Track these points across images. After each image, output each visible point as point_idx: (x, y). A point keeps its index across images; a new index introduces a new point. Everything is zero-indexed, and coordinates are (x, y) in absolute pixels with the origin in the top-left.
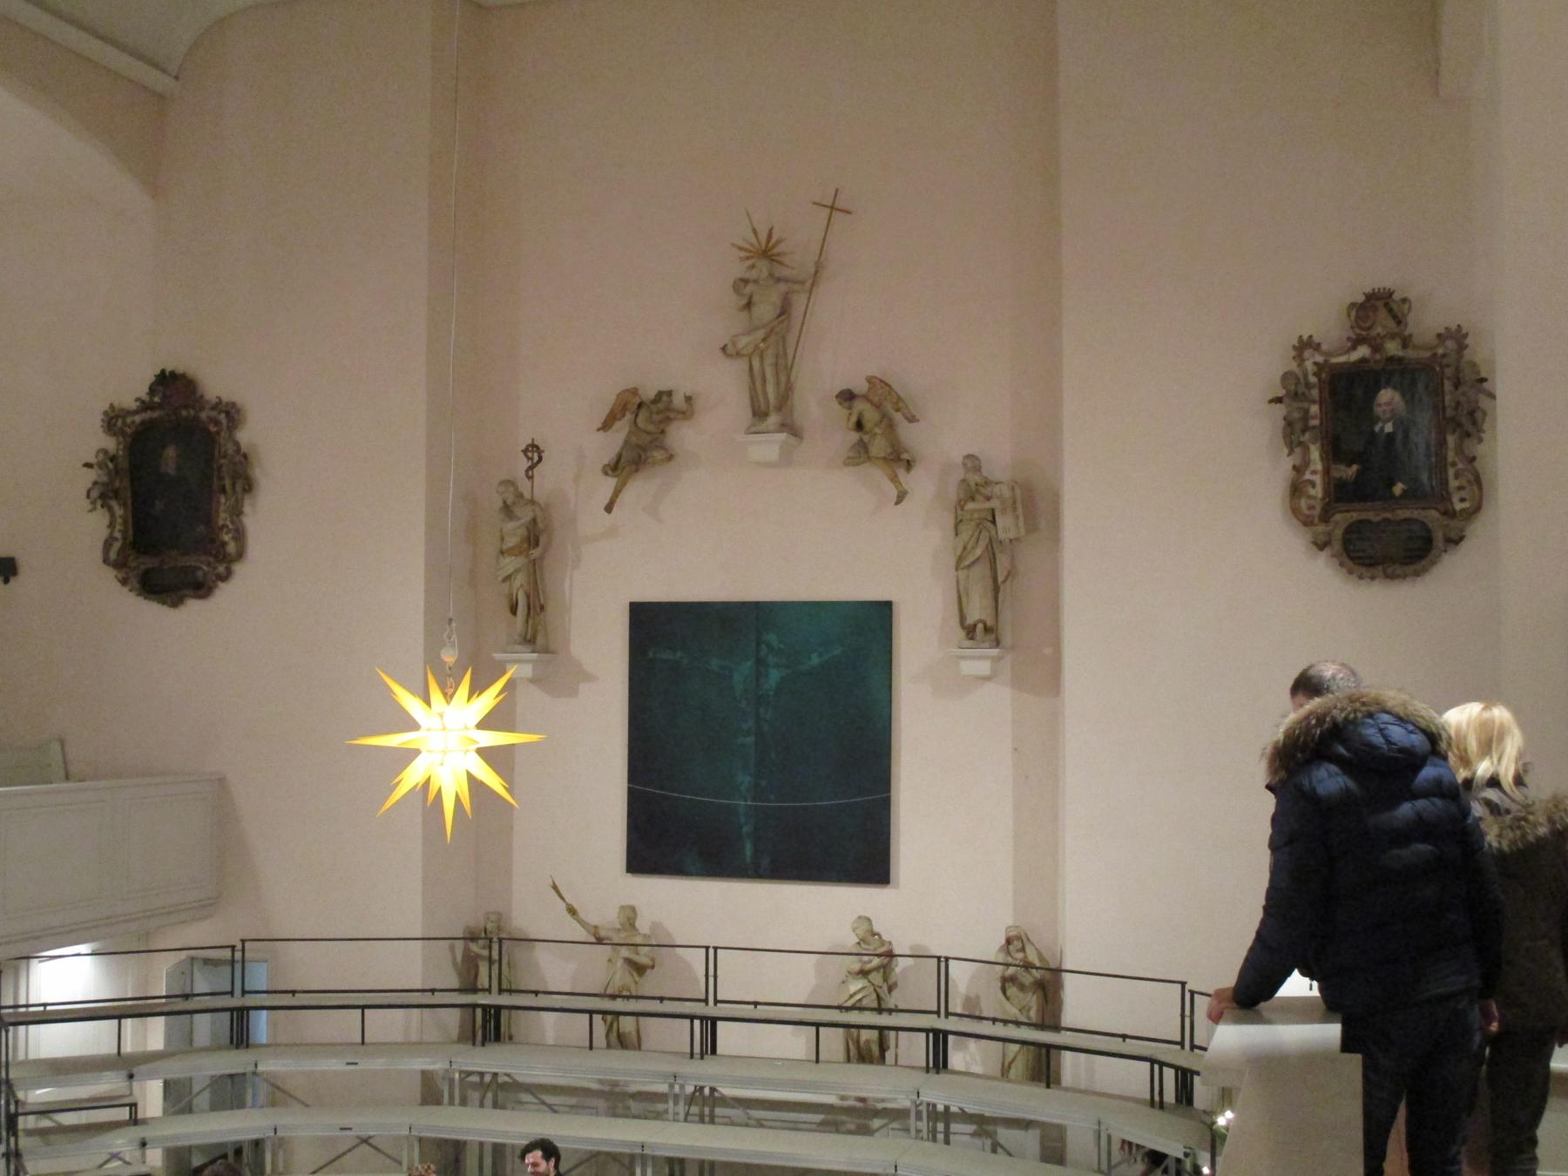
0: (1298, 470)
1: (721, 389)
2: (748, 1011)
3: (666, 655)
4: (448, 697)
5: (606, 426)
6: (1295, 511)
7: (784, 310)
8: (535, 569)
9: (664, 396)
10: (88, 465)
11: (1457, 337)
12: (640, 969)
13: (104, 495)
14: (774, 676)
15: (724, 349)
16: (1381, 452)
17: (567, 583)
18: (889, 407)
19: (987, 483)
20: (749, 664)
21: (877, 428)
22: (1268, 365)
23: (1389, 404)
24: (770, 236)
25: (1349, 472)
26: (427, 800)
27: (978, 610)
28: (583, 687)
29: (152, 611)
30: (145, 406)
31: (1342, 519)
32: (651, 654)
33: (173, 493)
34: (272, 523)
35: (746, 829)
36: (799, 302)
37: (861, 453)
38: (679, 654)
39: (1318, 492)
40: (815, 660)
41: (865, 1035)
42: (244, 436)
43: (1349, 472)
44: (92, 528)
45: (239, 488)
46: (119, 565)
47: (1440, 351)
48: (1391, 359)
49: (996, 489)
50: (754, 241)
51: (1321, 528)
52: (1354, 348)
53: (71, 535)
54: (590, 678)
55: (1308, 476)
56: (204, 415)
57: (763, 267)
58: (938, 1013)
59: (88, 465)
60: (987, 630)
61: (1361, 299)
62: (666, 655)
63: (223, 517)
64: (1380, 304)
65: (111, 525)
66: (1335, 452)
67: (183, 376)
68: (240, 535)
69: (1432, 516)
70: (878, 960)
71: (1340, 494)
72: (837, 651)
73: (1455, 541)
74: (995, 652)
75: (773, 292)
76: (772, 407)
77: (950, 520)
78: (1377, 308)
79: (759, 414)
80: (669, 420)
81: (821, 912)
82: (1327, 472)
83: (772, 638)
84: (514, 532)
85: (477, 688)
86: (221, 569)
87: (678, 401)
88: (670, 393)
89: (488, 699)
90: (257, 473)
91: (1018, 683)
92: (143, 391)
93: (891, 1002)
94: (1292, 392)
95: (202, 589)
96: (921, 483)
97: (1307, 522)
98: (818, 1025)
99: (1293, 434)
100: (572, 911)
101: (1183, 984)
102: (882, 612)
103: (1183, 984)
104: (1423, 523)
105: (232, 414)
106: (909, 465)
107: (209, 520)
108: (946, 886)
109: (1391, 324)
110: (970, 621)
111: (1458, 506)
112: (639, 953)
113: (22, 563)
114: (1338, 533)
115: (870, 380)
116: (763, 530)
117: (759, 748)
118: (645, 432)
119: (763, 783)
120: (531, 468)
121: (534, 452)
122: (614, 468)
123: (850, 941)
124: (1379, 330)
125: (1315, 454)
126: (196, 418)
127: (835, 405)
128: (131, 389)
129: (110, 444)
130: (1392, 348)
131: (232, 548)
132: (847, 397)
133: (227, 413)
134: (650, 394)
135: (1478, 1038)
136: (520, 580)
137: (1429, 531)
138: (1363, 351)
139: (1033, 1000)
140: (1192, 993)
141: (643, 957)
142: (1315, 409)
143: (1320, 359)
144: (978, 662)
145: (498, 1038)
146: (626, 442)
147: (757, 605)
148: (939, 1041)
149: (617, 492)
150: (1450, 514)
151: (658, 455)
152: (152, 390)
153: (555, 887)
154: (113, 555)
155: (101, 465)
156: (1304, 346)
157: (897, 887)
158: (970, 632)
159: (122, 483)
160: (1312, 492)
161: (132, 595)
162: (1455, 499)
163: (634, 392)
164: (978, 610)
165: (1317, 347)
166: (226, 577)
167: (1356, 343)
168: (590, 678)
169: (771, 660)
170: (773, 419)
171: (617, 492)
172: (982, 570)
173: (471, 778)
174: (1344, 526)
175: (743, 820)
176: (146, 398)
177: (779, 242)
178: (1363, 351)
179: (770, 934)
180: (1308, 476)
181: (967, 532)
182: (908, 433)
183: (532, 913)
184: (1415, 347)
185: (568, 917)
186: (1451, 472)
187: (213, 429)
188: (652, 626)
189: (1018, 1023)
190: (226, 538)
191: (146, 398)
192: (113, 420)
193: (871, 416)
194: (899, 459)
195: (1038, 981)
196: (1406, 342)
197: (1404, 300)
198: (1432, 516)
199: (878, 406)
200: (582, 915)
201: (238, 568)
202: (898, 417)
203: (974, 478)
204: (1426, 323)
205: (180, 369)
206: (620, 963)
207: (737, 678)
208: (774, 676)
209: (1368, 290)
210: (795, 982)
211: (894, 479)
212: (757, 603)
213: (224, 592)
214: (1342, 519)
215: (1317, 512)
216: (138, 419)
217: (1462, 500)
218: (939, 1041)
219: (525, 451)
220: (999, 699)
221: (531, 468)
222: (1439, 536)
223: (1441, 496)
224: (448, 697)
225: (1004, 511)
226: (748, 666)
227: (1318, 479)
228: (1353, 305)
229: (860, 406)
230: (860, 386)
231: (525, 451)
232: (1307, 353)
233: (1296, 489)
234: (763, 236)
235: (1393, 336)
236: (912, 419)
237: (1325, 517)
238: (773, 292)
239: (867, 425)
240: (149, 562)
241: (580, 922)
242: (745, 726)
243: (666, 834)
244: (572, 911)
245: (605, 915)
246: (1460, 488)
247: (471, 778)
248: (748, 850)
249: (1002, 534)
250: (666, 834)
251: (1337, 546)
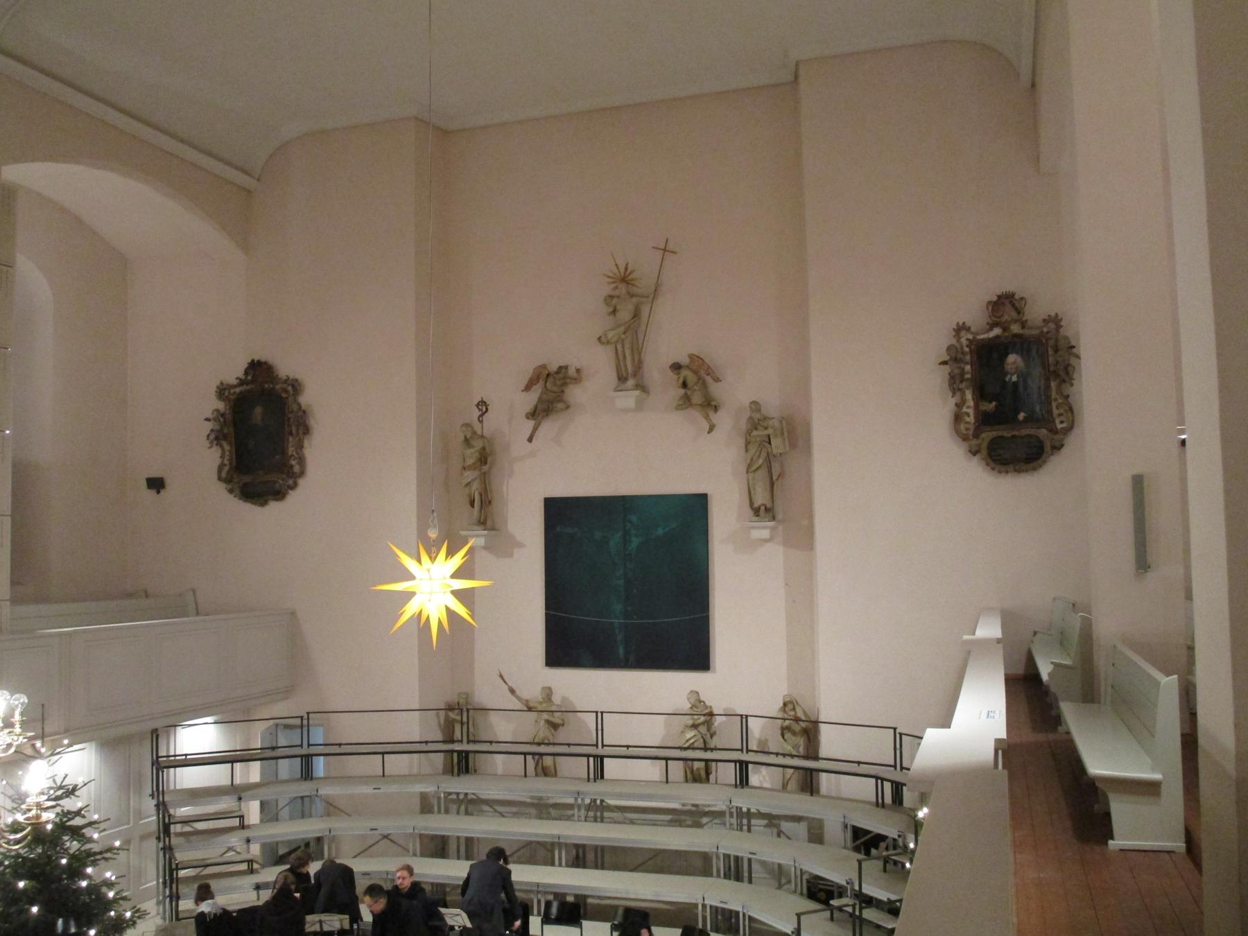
0: (959, 406)
1: (599, 365)
2: (623, 751)
3: (569, 530)
4: (433, 559)
5: (528, 388)
6: (957, 432)
7: (636, 315)
8: (485, 479)
9: (562, 369)
10: (208, 420)
11: (1056, 321)
12: (554, 726)
13: (218, 438)
14: (635, 542)
15: (599, 339)
16: (1012, 393)
17: (505, 489)
18: (702, 373)
19: (765, 418)
21: (696, 386)
22: (937, 341)
23: (1014, 363)
24: (626, 269)
25: (990, 406)
26: (420, 624)
27: (761, 498)
28: (516, 551)
29: (248, 509)
30: (242, 382)
31: (987, 435)
32: (558, 529)
33: (260, 435)
34: (322, 454)
35: (620, 637)
36: (645, 310)
37: (686, 402)
39: (971, 419)
40: (660, 531)
41: (697, 765)
42: (304, 399)
43: (990, 406)
44: (210, 459)
45: (301, 432)
46: (227, 481)
47: (1045, 330)
48: (1015, 336)
49: (771, 423)
50: (615, 270)
51: (975, 442)
52: (991, 329)
53: (200, 463)
54: (521, 545)
55: (965, 410)
56: (278, 387)
57: (623, 288)
58: (742, 750)
59: (208, 420)
60: (767, 510)
61: (995, 299)
62: (569, 530)
63: (291, 450)
64: (1007, 302)
65: (222, 457)
66: (981, 394)
67: (265, 363)
68: (302, 461)
69: (1043, 433)
70: (703, 718)
71: (985, 420)
72: (674, 525)
73: (1057, 448)
74: (772, 523)
75: (628, 303)
76: (630, 373)
77: (742, 442)
78: (1005, 305)
79: (622, 379)
80: (565, 384)
81: (667, 689)
82: (976, 407)
83: (634, 519)
84: (472, 455)
85: (451, 553)
86: (291, 482)
87: (572, 372)
88: (566, 367)
89: (458, 559)
90: (312, 422)
91: (788, 543)
92: (240, 373)
93: (713, 743)
94: (953, 358)
95: (279, 495)
96: (724, 420)
97: (965, 438)
98: (667, 759)
99: (955, 382)
100: (512, 691)
101: (895, 729)
102: (701, 501)
103: (895, 729)
104: (1037, 437)
105: (296, 386)
106: (716, 409)
107: (283, 452)
108: (745, 672)
109: (1014, 314)
110: (756, 505)
111: (1059, 426)
112: (553, 716)
113: (168, 481)
114: (985, 445)
115: (691, 356)
116: (624, 452)
117: (627, 587)
118: (551, 392)
120: (481, 415)
121: (483, 406)
122: (533, 415)
123: (686, 706)
124: (1006, 317)
125: (969, 395)
126: (273, 389)
127: (670, 373)
128: (233, 371)
129: (221, 406)
130: (1015, 328)
131: (297, 469)
132: (676, 367)
133: (293, 386)
134: (553, 368)
136: (476, 486)
137: (1041, 442)
138: (997, 331)
139: (801, 741)
140: (901, 734)
141: (557, 718)
142: (968, 368)
143: (970, 337)
144: (762, 531)
145: (467, 771)
146: (540, 400)
147: (624, 498)
148: (743, 767)
149: (535, 430)
150: (1054, 431)
151: (560, 406)
152: (246, 373)
153: (501, 676)
154: (224, 475)
155: (214, 419)
156: (960, 329)
157: (715, 672)
158: (756, 511)
159: (229, 430)
160: (968, 419)
161: (236, 500)
162: (1057, 421)
163: (544, 367)
164: (761, 498)
165: (968, 329)
166: (293, 487)
167: (992, 326)
168: (521, 545)
169: (633, 532)
170: (631, 382)
171: (535, 430)
172: (762, 473)
173: (448, 609)
174: (988, 440)
176: (243, 377)
177: (632, 272)
178: (997, 331)
179: (635, 703)
180: (965, 410)
181: (753, 450)
182: (714, 389)
183: (487, 693)
184: (1031, 328)
185: (509, 694)
186: (1054, 405)
187: (284, 395)
188: (561, 514)
189: (792, 756)
190: (293, 463)
191: (243, 377)
192: (222, 391)
193: (691, 379)
194: (710, 405)
195: (803, 729)
196: (1023, 325)
197: (1022, 299)
198: (1043, 433)
199: (696, 372)
200: (518, 692)
201: (301, 482)
202: (709, 379)
203: (757, 416)
204: (1036, 312)
205: (263, 360)
206: (542, 723)
207: (612, 543)
208: (635, 542)
209: (999, 293)
210: (652, 732)
211: (707, 417)
212: (623, 497)
213: (293, 496)
214: (987, 435)
215: (971, 432)
216: (238, 390)
217: (1062, 422)
218: (743, 767)
219: (477, 405)
220: (773, 556)
221: (481, 415)
222: (1048, 448)
223: (1046, 421)
224: (433, 559)
225: (776, 436)
227: (971, 411)
228: (989, 303)
229: (685, 373)
230: (685, 361)
231: (477, 405)
232: (963, 333)
233: (958, 418)
234: (622, 270)
235: (1016, 321)
236: (717, 380)
237: (976, 436)
238: (628, 303)
239: (690, 383)
240: (247, 479)
241: (518, 698)
243: (568, 643)
244: (512, 691)
245: (532, 692)
246: (1060, 415)
247: (448, 609)
248: (621, 651)
249: (775, 453)
250: (568, 643)
251: (984, 452)
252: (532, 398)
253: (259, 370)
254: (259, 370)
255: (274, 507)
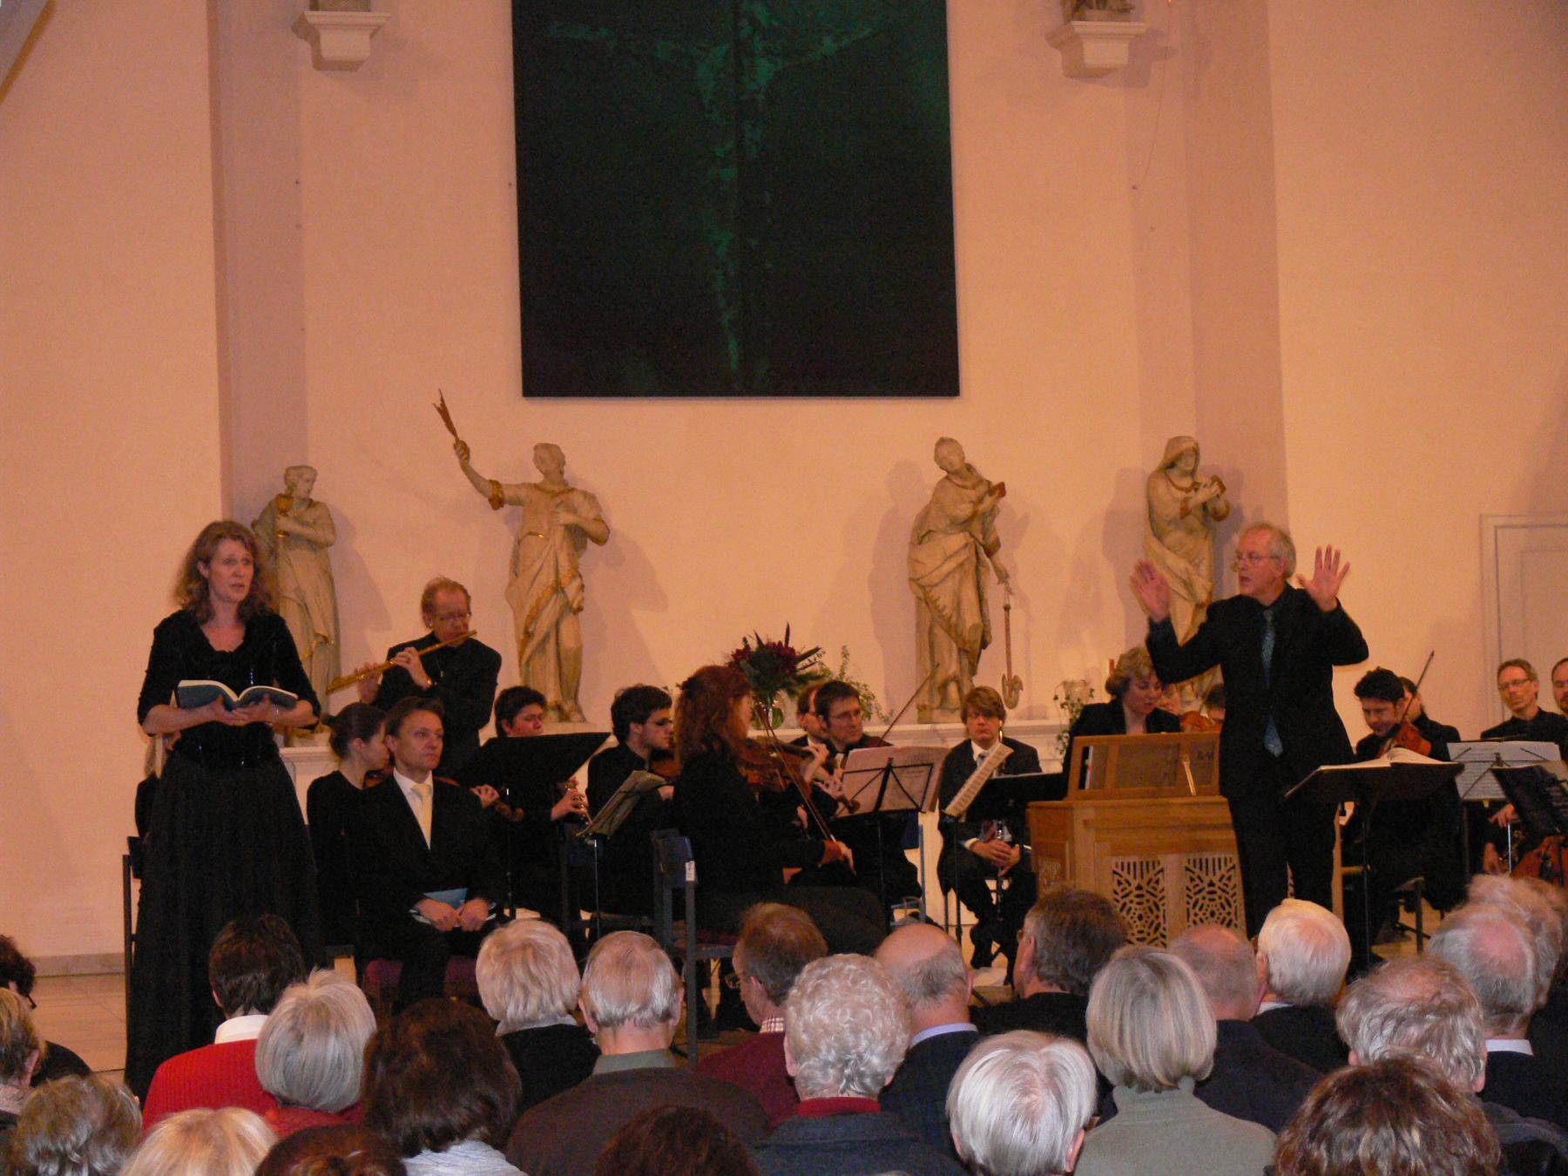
14: (764, 70)
20: (724, 48)
35: (726, 318)
38: (603, 32)
100: (462, 450)
119: (754, 242)
135: (818, 1074)
153: (443, 412)
169: (758, 44)
175: (722, 303)
208: (764, 70)
226: (721, 50)
242: (720, 152)
244: (462, 450)
245: (511, 463)
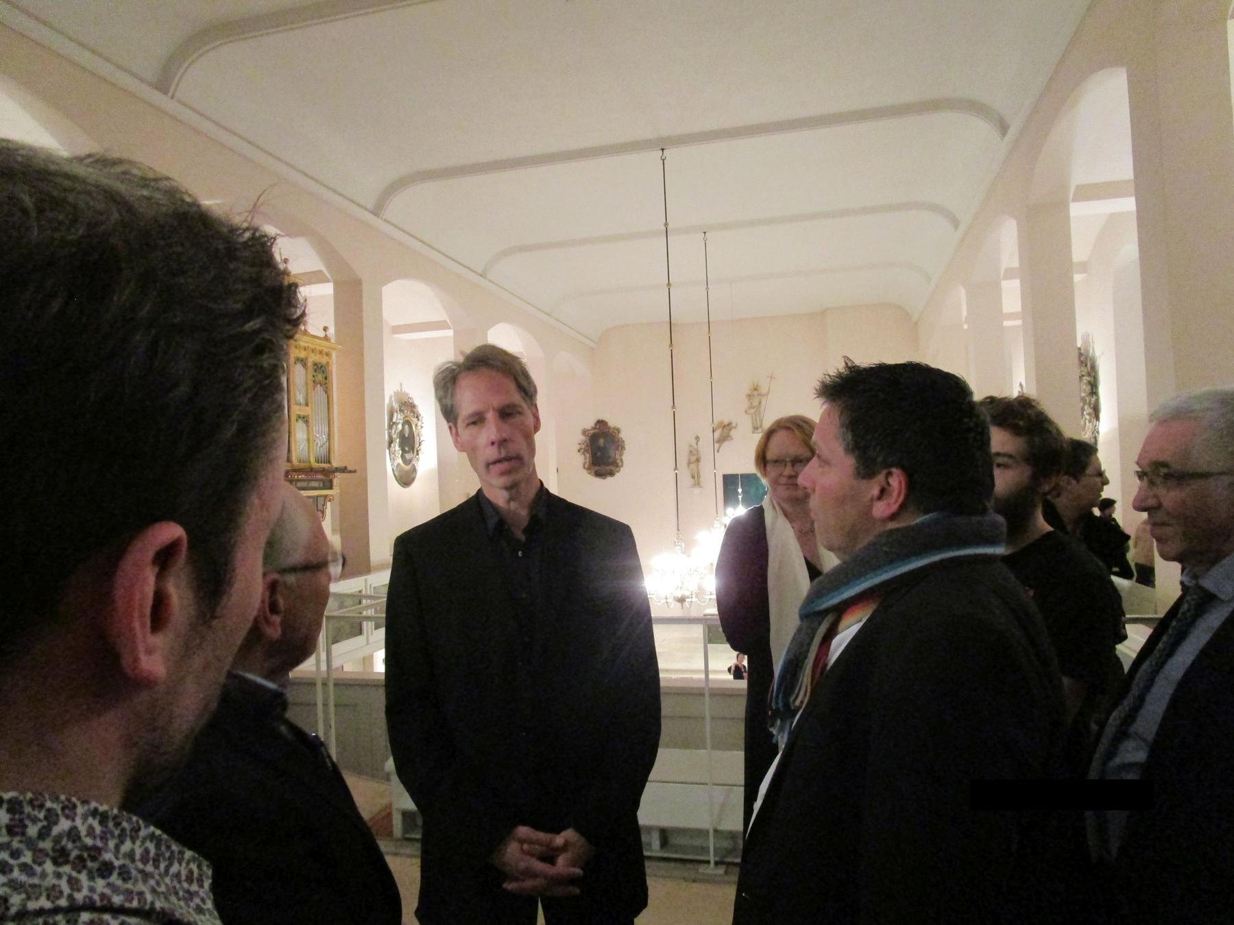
9: (729, 424)
29: (598, 480)
34: (629, 458)
36: (763, 401)
42: (623, 435)
46: (589, 469)
95: (612, 474)
105: (618, 430)
121: (697, 438)
128: (589, 424)
129: (583, 438)
134: (726, 422)
192: (584, 432)
213: (617, 475)
240: (597, 468)
252: (717, 434)
253: (601, 423)
254: (601, 423)
255: (609, 479)
